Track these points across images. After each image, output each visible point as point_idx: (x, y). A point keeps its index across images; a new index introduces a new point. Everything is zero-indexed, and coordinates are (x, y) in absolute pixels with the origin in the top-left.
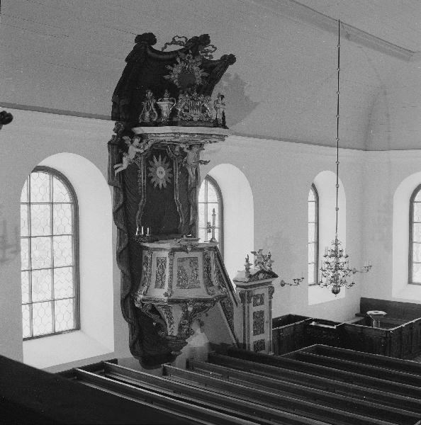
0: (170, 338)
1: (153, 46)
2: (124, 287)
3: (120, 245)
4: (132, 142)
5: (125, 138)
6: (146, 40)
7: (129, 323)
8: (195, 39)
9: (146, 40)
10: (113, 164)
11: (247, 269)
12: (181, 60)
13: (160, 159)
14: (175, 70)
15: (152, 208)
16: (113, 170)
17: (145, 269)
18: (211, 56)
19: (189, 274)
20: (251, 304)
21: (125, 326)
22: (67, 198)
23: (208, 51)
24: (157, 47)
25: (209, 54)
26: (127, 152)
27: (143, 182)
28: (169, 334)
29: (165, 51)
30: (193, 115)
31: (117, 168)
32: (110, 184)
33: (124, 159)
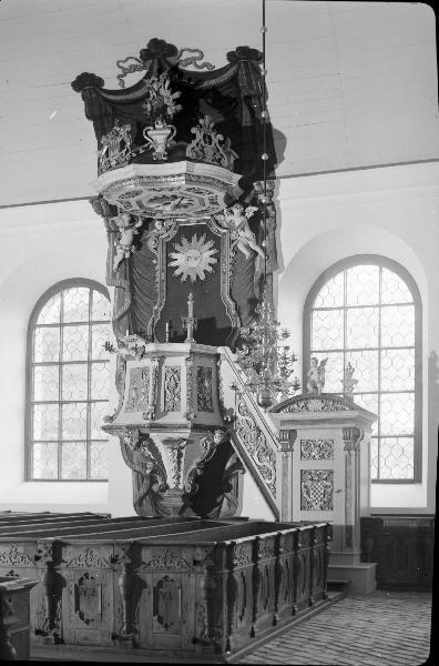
6: (87, 84)
8: (146, 55)
9: (87, 84)
24: (111, 84)
25: (199, 63)
27: (160, 276)
29: (127, 86)
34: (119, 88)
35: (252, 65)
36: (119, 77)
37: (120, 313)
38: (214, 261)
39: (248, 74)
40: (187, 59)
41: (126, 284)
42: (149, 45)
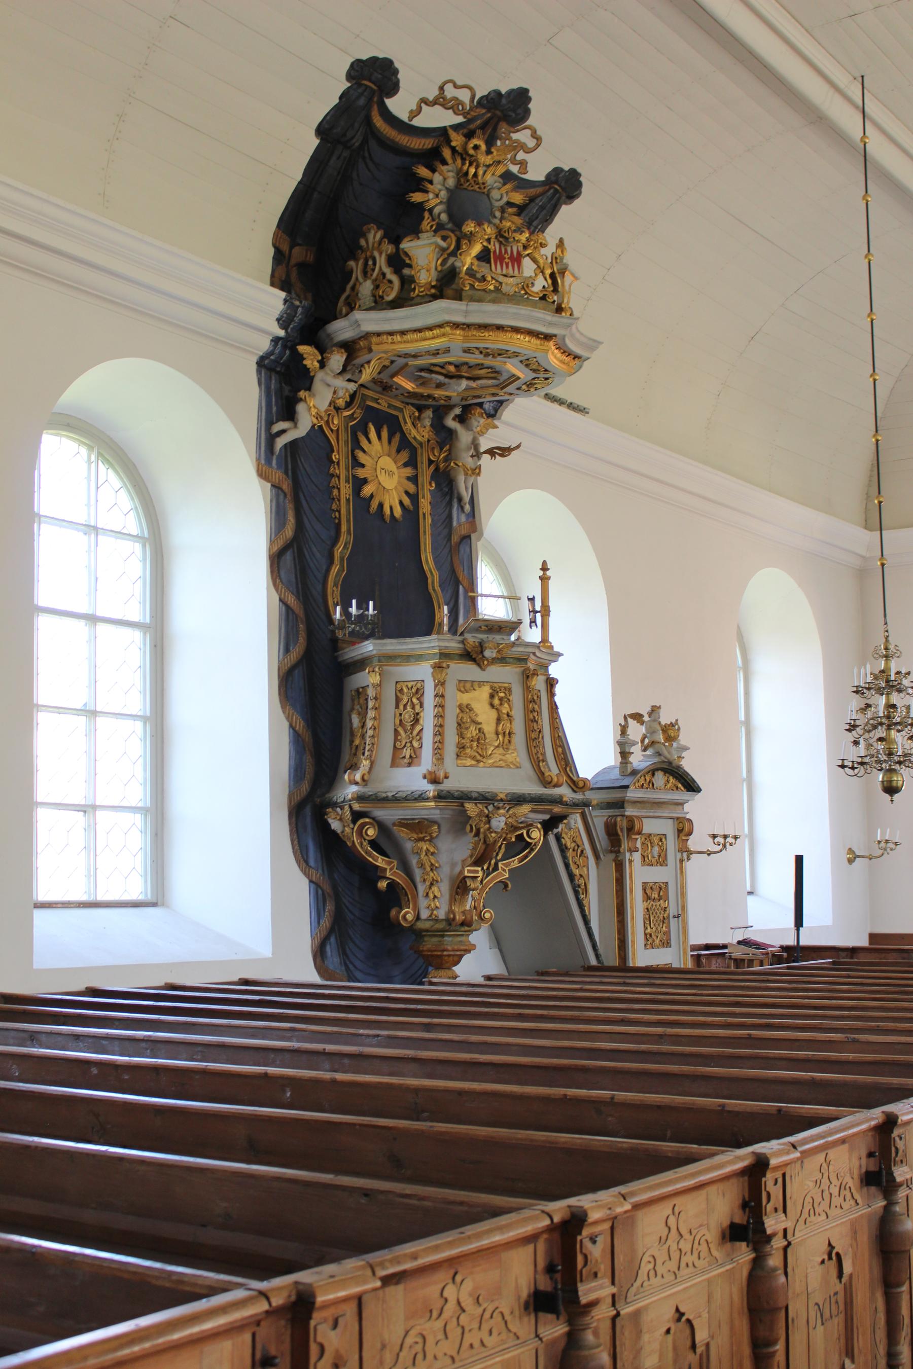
0: (427, 925)
1: (390, 103)
2: (297, 773)
3: (287, 650)
4: (322, 364)
5: (303, 349)
6: (373, 78)
7: (311, 881)
8: (493, 101)
9: (373, 78)
10: (270, 423)
11: (624, 755)
12: (454, 150)
13: (385, 434)
14: (437, 178)
15: (365, 576)
16: (271, 439)
17: (356, 721)
18: (523, 164)
19: (489, 727)
20: (637, 856)
21: (300, 889)
22: (133, 524)
23: (522, 147)
25: (521, 156)
26: (309, 389)
28: (424, 914)
29: (418, 122)
30: (501, 279)
31: (283, 432)
32: (261, 475)
33: (301, 408)
34: (404, 117)
35: (559, 199)
36: (424, 101)
37: (280, 543)
38: (412, 488)
39: (542, 208)
40: (517, 141)
41: (286, 486)
42: (511, 92)
